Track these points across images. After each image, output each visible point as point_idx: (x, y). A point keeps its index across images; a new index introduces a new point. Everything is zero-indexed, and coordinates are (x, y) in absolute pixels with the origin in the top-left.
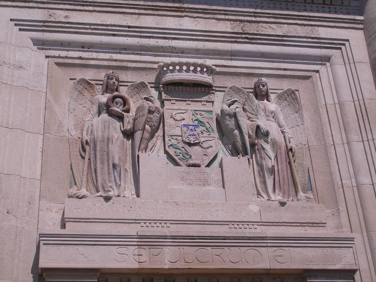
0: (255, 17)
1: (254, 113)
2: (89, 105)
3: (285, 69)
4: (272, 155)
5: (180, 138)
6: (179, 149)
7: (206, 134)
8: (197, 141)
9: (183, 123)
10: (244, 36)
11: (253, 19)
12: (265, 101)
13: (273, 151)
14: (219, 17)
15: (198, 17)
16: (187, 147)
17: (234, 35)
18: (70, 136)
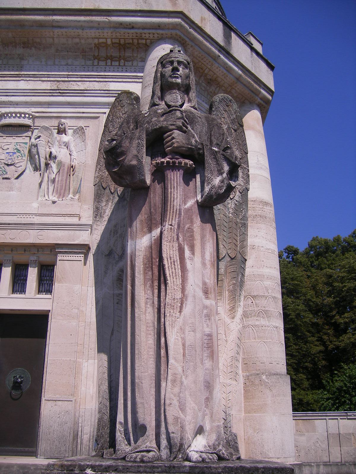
0: (68, 78)
3: (83, 113)
4: (55, 170)
5: (2, 161)
7: (20, 158)
8: (13, 163)
9: (8, 151)
10: (58, 91)
11: (66, 79)
12: (64, 135)
13: (57, 168)
14: (43, 79)
15: (30, 80)
16: (6, 167)
17: (51, 91)
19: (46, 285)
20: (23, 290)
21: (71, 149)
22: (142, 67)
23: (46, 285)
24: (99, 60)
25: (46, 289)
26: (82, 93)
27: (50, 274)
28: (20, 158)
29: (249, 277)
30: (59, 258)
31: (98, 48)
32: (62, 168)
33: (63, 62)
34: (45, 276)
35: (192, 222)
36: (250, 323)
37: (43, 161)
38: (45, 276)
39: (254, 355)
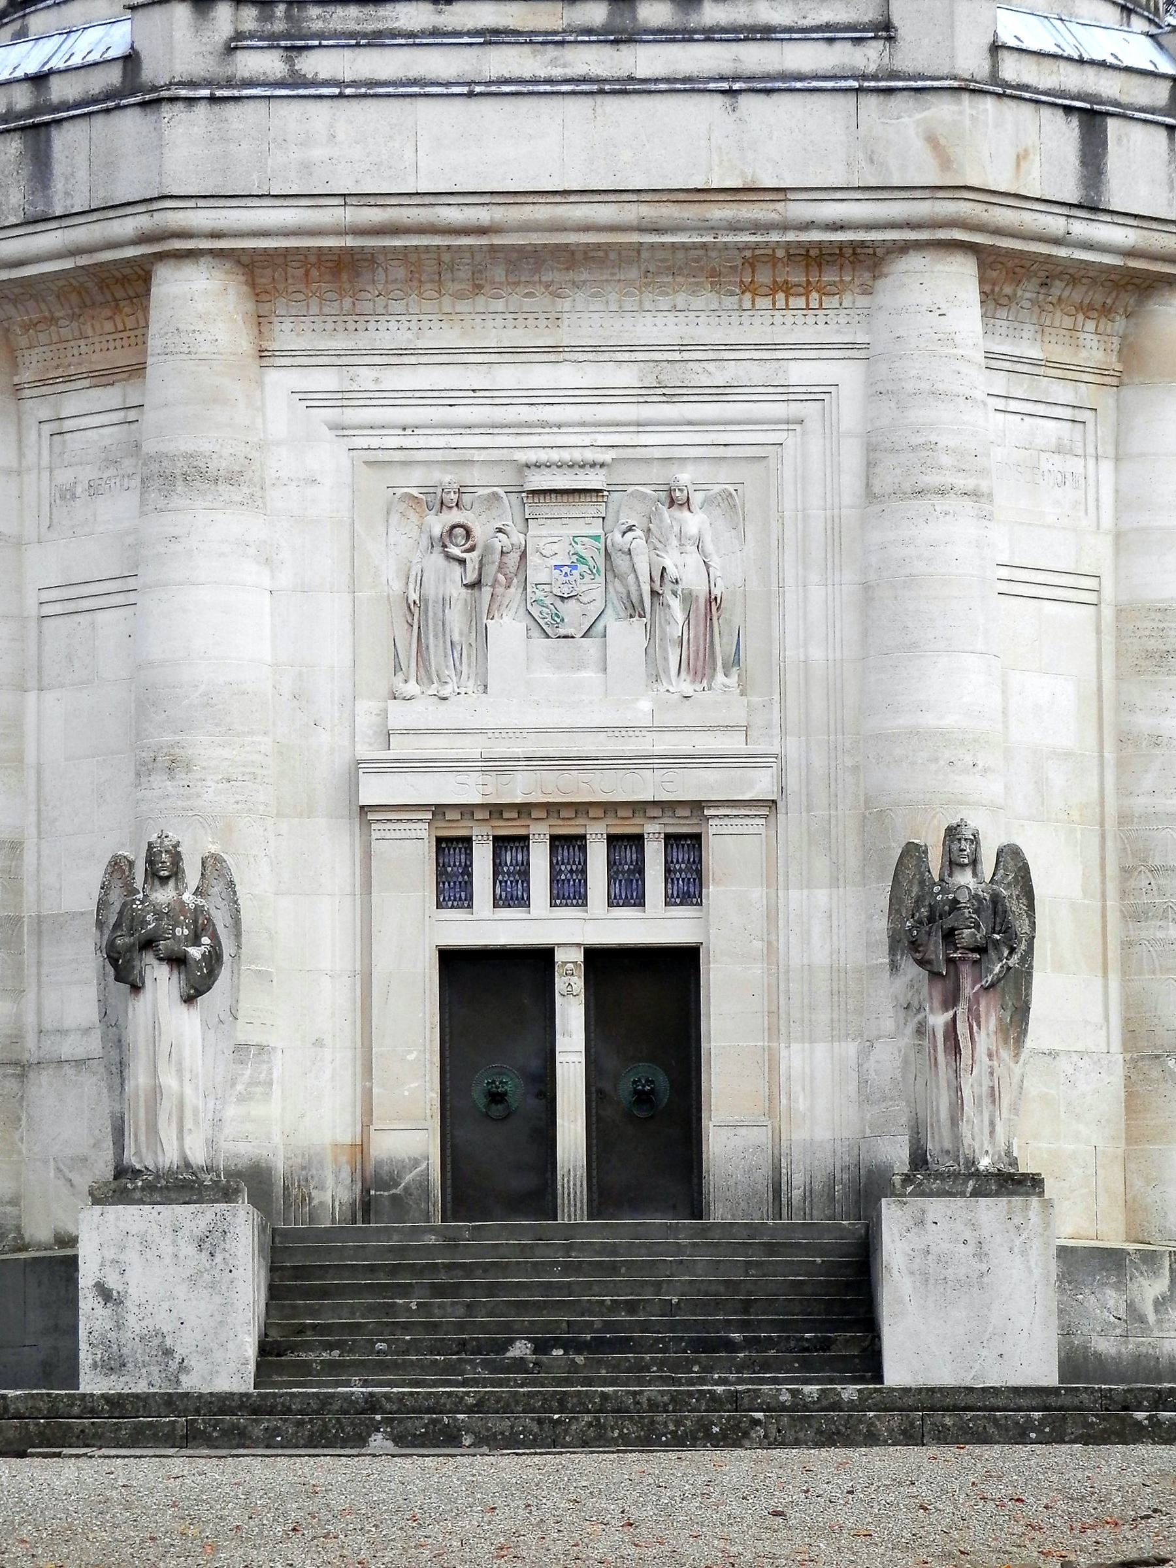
1: (662, 540)
2: (415, 533)
4: (680, 616)
5: (547, 588)
6: (547, 607)
10: (659, 391)
11: (677, 356)
13: (684, 609)
16: (559, 603)
18: (391, 592)
19: (681, 882)
20: (640, 902)
21: (705, 548)
22: (866, 311)
23: (681, 882)
24: (755, 294)
25: (681, 891)
26: (720, 393)
27: (686, 856)
28: (587, 578)
29: (1143, 818)
30: (711, 831)
31: (752, 266)
32: (694, 607)
33: (664, 302)
34: (675, 860)
35: (978, 1004)
36: (1144, 934)
37: (646, 589)
38: (675, 860)
39: (1151, 1011)
